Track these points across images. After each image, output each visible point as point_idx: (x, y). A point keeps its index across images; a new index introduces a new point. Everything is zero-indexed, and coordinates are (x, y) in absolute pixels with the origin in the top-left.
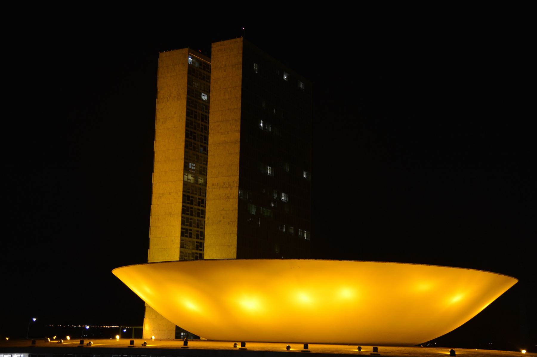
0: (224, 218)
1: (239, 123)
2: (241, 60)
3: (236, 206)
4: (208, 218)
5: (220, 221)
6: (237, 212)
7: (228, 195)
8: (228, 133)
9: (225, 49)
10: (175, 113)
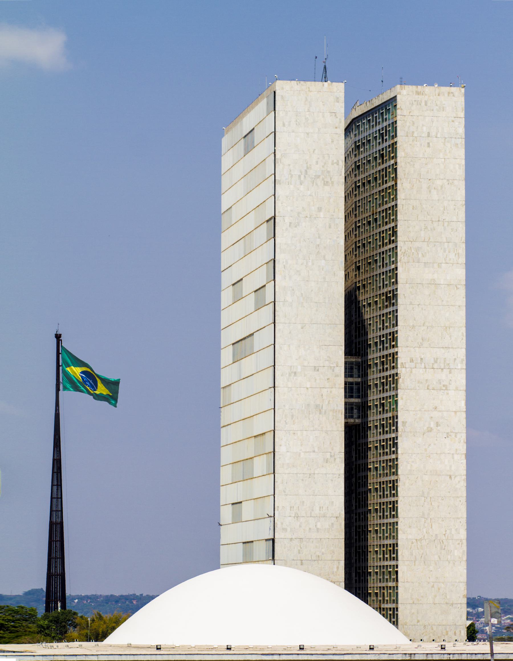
0: (437, 425)
2: (461, 130)
3: (463, 404)
4: (404, 423)
6: (464, 415)
7: (445, 383)
8: (439, 265)
9: (426, 105)
10: (320, 209)
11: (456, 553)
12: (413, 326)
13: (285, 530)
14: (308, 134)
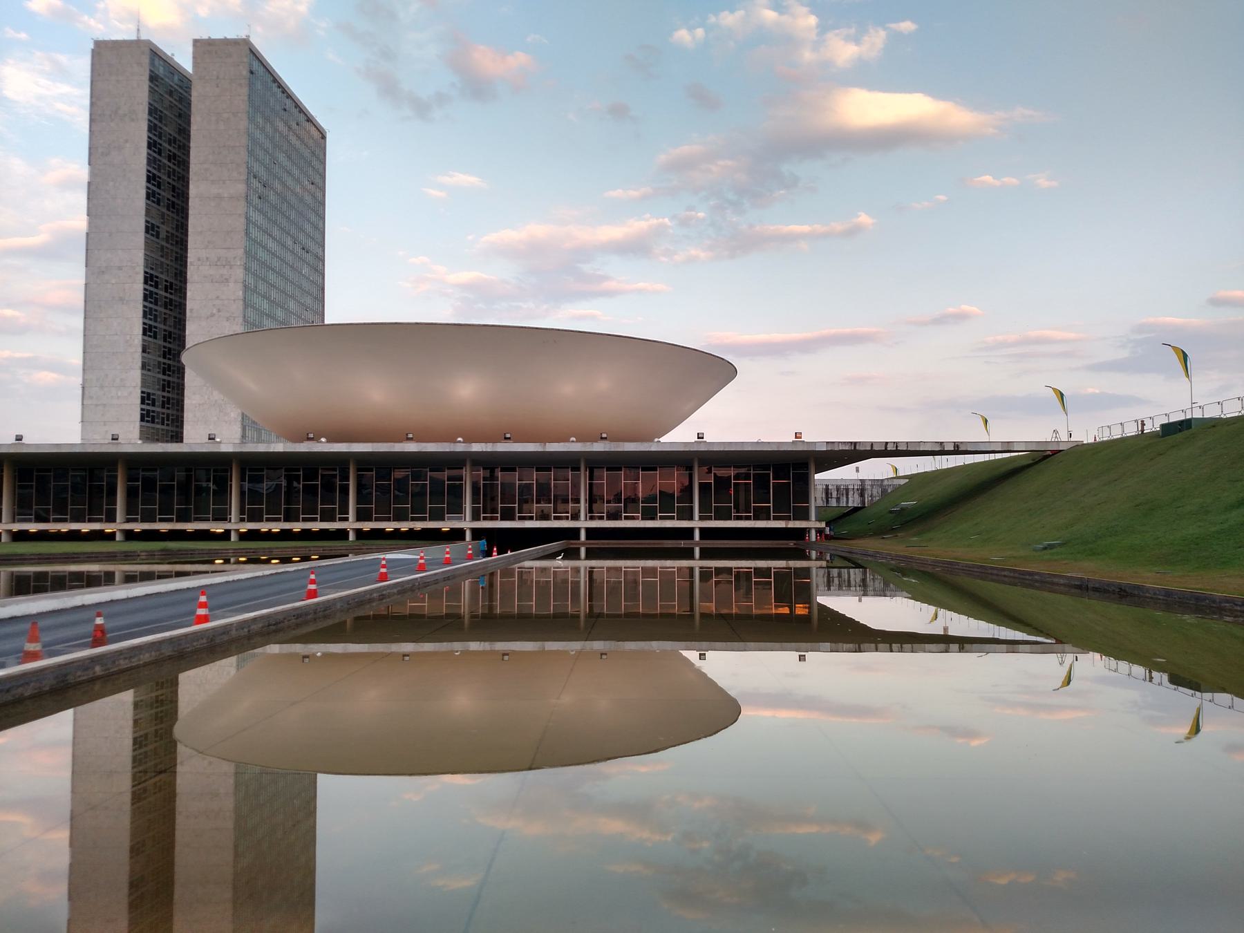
0: (219, 311)
1: (244, 170)
5: (213, 315)
11: (232, 415)
12: (201, 232)
13: (91, 398)
14: (118, 81)
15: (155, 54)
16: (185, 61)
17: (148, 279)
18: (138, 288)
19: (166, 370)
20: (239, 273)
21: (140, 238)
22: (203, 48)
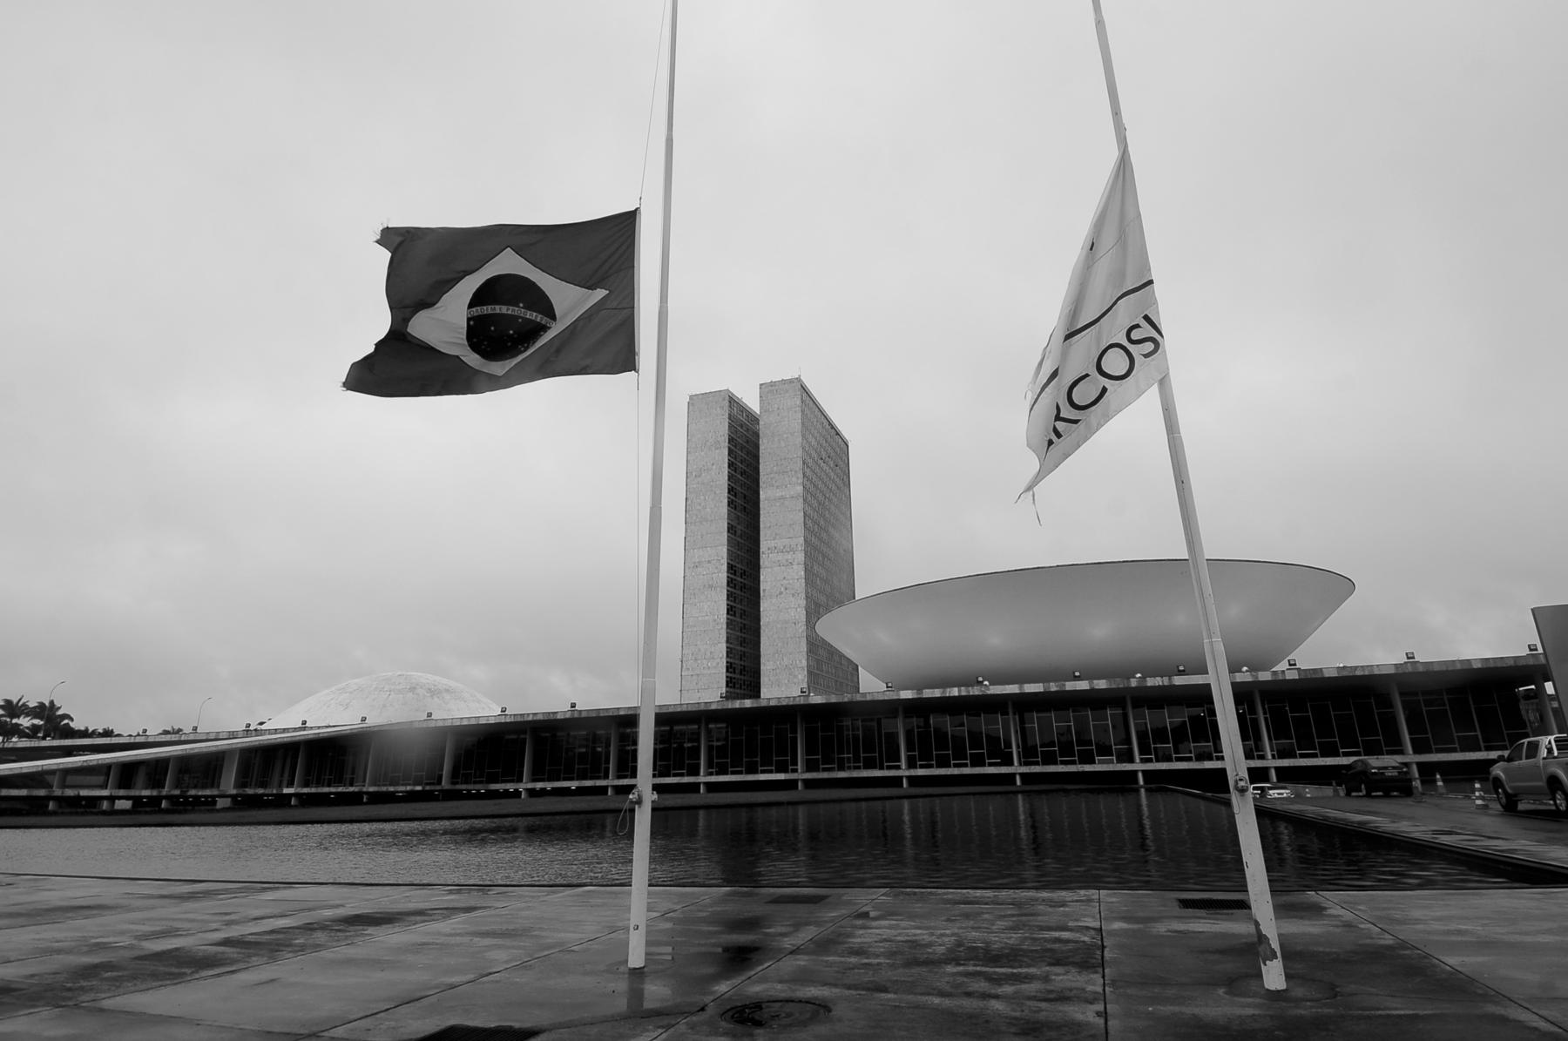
15: (733, 401)
16: (753, 403)
17: (731, 568)
18: (723, 576)
19: (743, 642)
20: (801, 556)
21: (724, 537)
22: (768, 390)
